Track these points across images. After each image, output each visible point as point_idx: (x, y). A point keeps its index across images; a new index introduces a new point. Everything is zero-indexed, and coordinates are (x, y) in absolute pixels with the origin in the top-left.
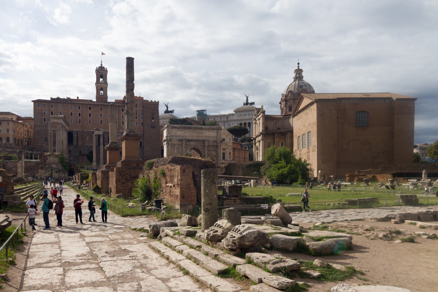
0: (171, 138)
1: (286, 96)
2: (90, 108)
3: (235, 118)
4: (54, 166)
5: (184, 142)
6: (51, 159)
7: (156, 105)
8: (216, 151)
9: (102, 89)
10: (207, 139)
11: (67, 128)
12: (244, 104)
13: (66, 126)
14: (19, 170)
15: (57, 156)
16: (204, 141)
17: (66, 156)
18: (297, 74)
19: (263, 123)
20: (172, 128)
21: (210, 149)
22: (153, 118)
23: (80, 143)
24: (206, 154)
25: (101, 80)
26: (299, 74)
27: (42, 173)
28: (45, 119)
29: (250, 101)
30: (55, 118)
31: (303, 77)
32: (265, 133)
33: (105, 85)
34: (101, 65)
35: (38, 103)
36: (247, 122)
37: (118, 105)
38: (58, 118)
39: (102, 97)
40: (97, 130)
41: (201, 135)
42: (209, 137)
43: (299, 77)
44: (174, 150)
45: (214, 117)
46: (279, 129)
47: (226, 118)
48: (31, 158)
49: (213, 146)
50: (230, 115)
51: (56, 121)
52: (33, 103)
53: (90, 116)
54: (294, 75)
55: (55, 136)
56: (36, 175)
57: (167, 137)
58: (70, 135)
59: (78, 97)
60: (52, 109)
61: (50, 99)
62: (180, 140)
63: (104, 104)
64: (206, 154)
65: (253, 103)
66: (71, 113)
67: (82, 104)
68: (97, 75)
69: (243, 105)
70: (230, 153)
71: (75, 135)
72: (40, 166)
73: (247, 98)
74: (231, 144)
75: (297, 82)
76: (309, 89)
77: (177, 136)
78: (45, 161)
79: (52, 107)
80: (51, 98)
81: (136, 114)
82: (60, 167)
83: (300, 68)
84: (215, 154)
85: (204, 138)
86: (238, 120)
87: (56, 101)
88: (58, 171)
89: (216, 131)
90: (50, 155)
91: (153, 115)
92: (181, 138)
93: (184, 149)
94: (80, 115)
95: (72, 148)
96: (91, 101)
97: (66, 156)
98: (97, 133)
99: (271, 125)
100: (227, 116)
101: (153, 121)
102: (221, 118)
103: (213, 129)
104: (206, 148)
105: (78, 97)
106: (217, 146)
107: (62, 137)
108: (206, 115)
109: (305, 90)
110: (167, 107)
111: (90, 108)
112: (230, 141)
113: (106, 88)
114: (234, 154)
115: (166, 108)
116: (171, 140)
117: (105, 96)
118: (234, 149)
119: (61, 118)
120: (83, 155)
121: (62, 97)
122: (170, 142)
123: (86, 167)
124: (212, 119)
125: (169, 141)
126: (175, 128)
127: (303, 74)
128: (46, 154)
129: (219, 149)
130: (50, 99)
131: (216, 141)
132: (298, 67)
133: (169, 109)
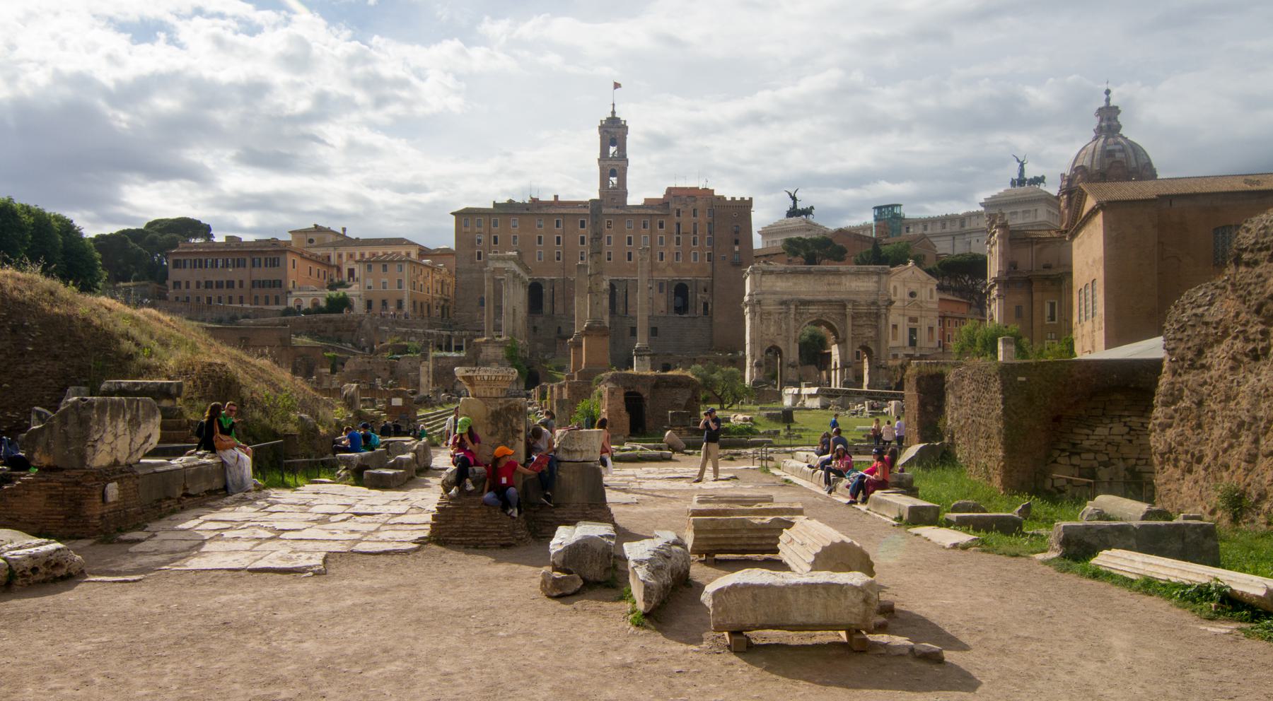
0: (760, 297)
1: (1070, 180)
5: (793, 307)
7: (744, 207)
8: (876, 327)
9: (613, 173)
10: (853, 297)
11: (527, 278)
12: (1013, 183)
13: (523, 274)
14: (423, 380)
15: (501, 345)
16: (842, 304)
17: (521, 342)
18: (1102, 120)
19: (1002, 254)
20: (764, 273)
21: (861, 323)
22: (737, 242)
23: (559, 308)
24: (850, 335)
25: (612, 149)
26: (1109, 119)
28: (479, 254)
29: (1029, 174)
30: (498, 259)
31: (1120, 127)
32: (1006, 278)
34: (613, 112)
35: (465, 217)
37: (650, 212)
38: (504, 259)
39: (613, 192)
41: (834, 288)
42: (858, 293)
43: (1109, 126)
44: (768, 327)
45: (925, 222)
46: (1048, 267)
47: (958, 224)
48: (448, 349)
49: (868, 315)
50: (969, 216)
51: (499, 265)
54: (1095, 122)
55: (498, 293)
57: (750, 295)
58: (535, 292)
59: (556, 197)
60: (496, 231)
62: (783, 303)
64: (850, 335)
65: (1040, 180)
66: (540, 238)
68: (602, 138)
69: (1009, 187)
70: (931, 329)
71: (546, 291)
73: (1022, 165)
74: (936, 306)
75: (1102, 140)
76: (1133, 159)
77: (775, 293)
79: (495, 225)
80: (495, 204)
81: (695, 232)
83: (1112, 103)
84: (872, 334)
85: (843, 297)
87: (507, 210)
89: (875, 278)
90: (487, 342)
91: (737, 232)
92: (785, 297)
93: (792, 323)
94: (558, 242)
95: (539, 320)
97: (521, 342)
99: (1025, 258)
100: (962, 219)
101: (737, 248)
102: (944, 226)
103: (868, 273)
104: (849, 321)
105: (556, 197)
106: (878, 316)
107: (516, 299)
108: (898, 218)
109: (1120, 162)
110: (794, 199)
112: (931, 297)
113: (625, 169)
115: (791, 202)
116: (759, 302)
117: (621, 191)
118: (943, 318)
119: (511, 258)
121: (518, 200)
122: (758, 309)
124: (915, 231)
125: (756, 304)
126: (771, 272)
127: (1120, 118)
128: (477, 340)
129: (883, 321)
131: (874, 303)
132: (1108, 100)
133: (800, 206)
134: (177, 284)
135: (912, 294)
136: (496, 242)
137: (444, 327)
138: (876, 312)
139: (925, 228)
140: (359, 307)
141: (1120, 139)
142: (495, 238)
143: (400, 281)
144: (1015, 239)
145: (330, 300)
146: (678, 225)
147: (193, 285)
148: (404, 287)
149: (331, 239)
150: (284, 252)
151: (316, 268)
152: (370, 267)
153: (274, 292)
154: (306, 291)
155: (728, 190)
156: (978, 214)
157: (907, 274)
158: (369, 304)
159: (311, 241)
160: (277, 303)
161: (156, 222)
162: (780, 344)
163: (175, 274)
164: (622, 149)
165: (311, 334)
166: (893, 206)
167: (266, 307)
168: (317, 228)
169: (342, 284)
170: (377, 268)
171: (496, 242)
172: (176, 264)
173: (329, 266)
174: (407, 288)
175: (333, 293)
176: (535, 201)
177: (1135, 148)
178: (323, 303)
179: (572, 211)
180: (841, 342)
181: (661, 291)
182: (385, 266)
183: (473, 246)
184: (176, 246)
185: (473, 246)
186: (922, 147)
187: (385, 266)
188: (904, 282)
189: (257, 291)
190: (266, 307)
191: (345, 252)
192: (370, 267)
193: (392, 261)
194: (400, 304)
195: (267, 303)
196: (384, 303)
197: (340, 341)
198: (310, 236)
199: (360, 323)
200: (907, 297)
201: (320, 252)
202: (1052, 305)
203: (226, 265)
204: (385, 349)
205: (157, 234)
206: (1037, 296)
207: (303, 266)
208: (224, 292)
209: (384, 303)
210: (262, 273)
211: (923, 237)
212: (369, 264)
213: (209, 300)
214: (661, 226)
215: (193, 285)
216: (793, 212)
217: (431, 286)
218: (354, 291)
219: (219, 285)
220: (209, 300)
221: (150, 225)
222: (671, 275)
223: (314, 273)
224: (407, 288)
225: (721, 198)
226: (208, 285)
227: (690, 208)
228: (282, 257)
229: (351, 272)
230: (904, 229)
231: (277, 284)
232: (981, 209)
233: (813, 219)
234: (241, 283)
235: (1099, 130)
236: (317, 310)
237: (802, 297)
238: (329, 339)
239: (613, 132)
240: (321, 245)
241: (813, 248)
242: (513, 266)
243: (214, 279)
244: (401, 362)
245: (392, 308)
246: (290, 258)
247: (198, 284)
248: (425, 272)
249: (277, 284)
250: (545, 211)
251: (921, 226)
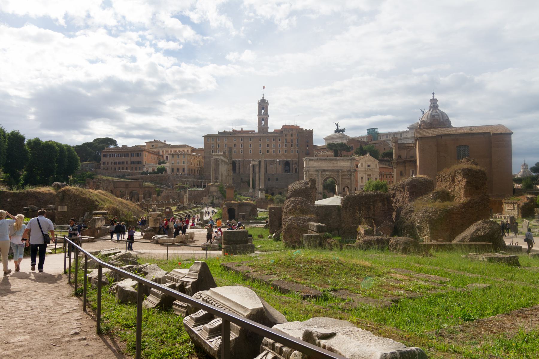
2: (251, 140)
4: (215, 194)
5: (320, 172)
6: (213, 189)
7: (310, 133)
8: (351, 179)
9: (263, 120)
10: (341, 168)
14: (185, 200)
15: (217, 186)
16: (338, 171)
20: (310, 160)
22: (307, 146)
24: (340, 182)
27: (206, 200)
30: (216, 155)
33: (266, 116)
34: (263, 98)
35: (208, 138)
37: (275, 135)
38: (218, 155)
40: (253, 160)
41: (334, 165)
43: (434, 106)
48: (201, 187)
50: (404, 132)
51: (216, 157)
53: (250, 146)
56: (202, 201)
59: (242, 129)
60: (219, 142)
61: (217, 133)
62: (317, 171)
63: (265, 135)
64: (340, 182)
72: (205, 194)
76: (441, 118)
77: (314, 167)
78: (208, 190)
80: (219, 133)
82: (220, 195)
83: (435, 97)
85: (338, 168)
87: (224, 135)
88: (218, 198)
89: (350, 162)
90: (212, 185)
91: (307, 142)
92: (317, 169)
93: (320, 178)
96: (253, 132)
98: (253, 163)
101: (307, 148)
103: (347, 160)
105: (242, 129)
106: (351, 175)
107: (224, 169)
108: (377, 133)
110: (337, 126)
111: (251, 140)
113: (268, 119)
115: (336, 127)
116: (308, 170)
117: (266, 127)
118: (381, 175)
119: (221, 155)
120: (244, 182)
121: (227, 131)
122: (307, 173)
123: (244, 193)
124: (383, 138)
126: (312, 160)
127: (438, 103)
130: (217, 133)
131: (349, 171)
132: (433, 96)
133: (340, 128)
134: (104, 163)
135: (369, 166)
137: (200, 178)
138: (352, 173)
139: (387, 137)
140: (169, 171)
141: (437, 111)
143: (184, 161)
144: (401, 147)
145: (158, 169)
146: (286, 140)
147: (110, 163)
148: (184, 163)
149: (160, 145)
150: (143, 151)
151: (154, 156)
152: (173, 156)
153: (138, 166)
154: (150, 165)
155: (305, 126)
156: (407, 132)
157: (367, 158)
158: (173, 170)
159: (153, 146)
160: (140, 170)
161: (97, 139)
163: (103, 160)
164: (266, 111)
165: (151, 182)
166: (374, 129)
167: (136, 171)
168: (155, 141)
169: (164, 163)
170: (176, 157)
172: (104, 156)
173: (159, 155)
174: (186, 164)
175: (160, 166)
177: (443, 114)
178: (156, 170)
179: (247, 135)
180: (338, 185)
181: (279, 164)
182: (178, 156)
184: (104, 149)
186: (397, 101)
187: (178, 156)
188: (365, 161)
189: (133, 165)
190: (136, 171)
191: (165, 150)
192: (173, 156)
193: (181, 154)
194: (184, 170)
195: (136, 170)
196: (178, 169)
197: (161, 184)
198: (152, 144)
199: (169, 177)
200: (367, 167)
201: (156, 150)
202: (413, 171)
203: (122, 156)
204: (176, 188)
205: (97, 144)
206: (407, 168)
207: (149, 156)
208: (121, 166)
209: (178, 169)
210: (135, 159)
211: (384, 141)
212: (173, 155)
213: (115, 169)
214: (279, 140)
215: (110, 163)
216: (337, 131)
217: (195, 163)
218: (167, 165)
219: (119, 163)
220: (115, 169)
221: (95, 140)
222: (283, 158)
223: (153, 158)
224: (186, 164)
225: (302, 129)
226: (115, 163)
227: (290, 133)
228: (142, 153)
229: (167, 157)
230: (379, 138)
231: (140, 163)
232: (408, 130)
233: (346, 133)
234: (127, 162)
235: (431, 107)
236: (154, 172)
237: (324, 168)
238: (158, 183)
239: (263, 105)
240: (156, 148)
241: (340, 147)
242: (222, 158)
243: (117, 161)
245: (181, 171)
246: (145, 153)
247: (112, 163)
248: (193, 158)
249: (140, 163)
250: (237, 135)
251: (385, 136)
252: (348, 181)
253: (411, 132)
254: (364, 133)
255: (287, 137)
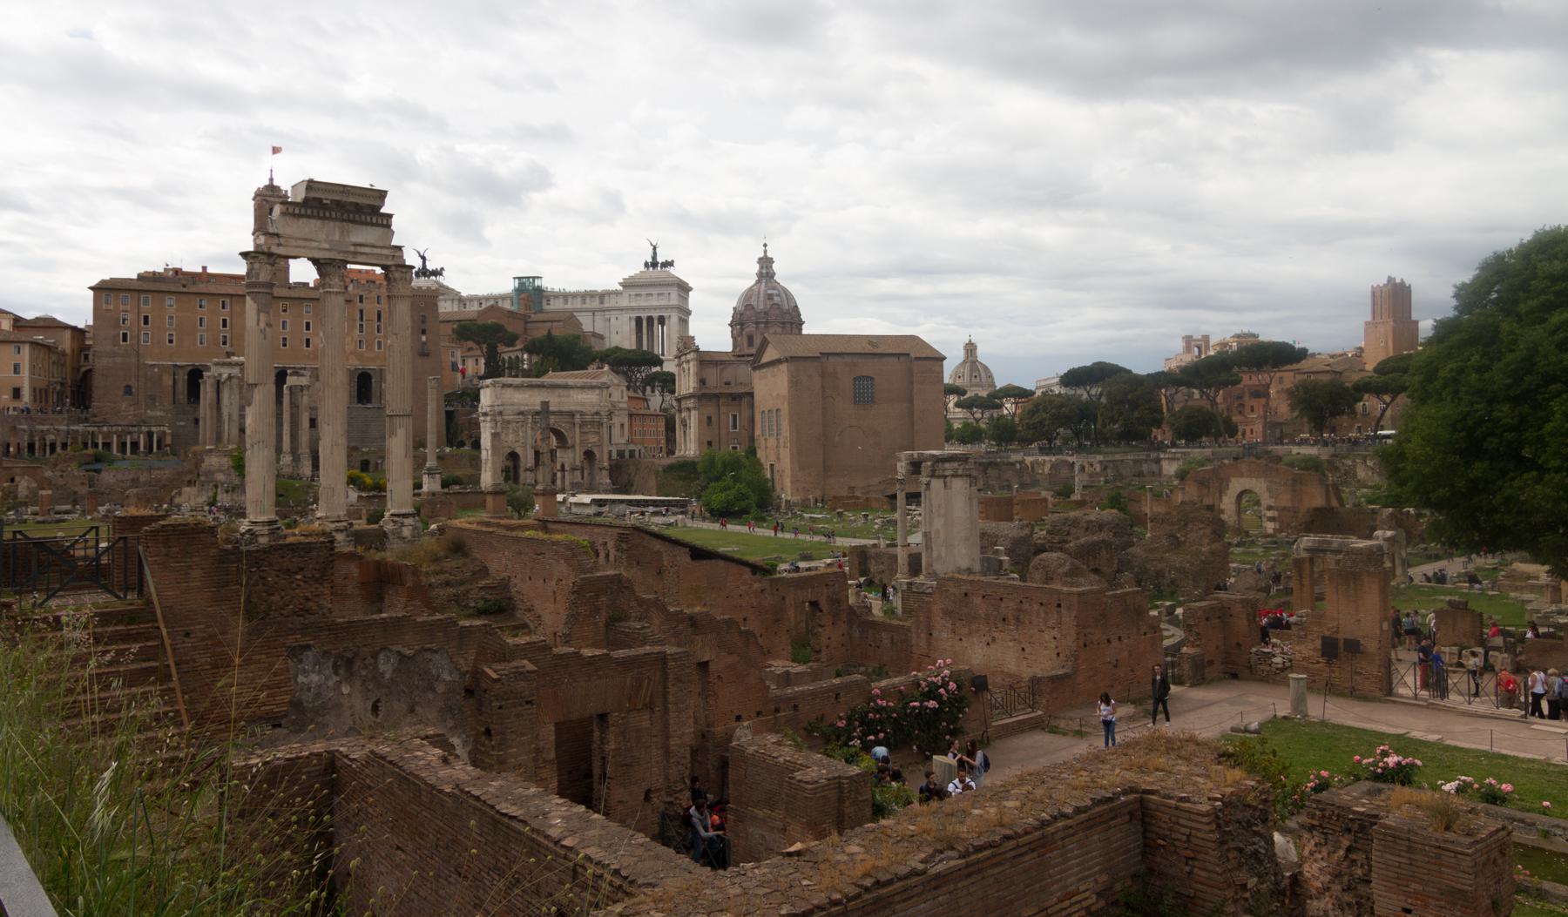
3: (624, 302)
10: (579, 408)
12: (646, 265)
16: (572, 414)
20: (504, 386)
22: (424, 332)
28: (125, 335)
35: (103, 290)
36: (655, 315)
42: (583, 404)
47: (597, 300)
52: (91, 293)
59: (204, 268)
60: (146, 309)
62: (521, 413)
65: (669, 264)
67: (232, 295)
69: (642, 268)
72: (188, 478)
78: (197, 466)
79: (146, 303)
85: (573, 408)
86: (632, 309)
94: (225, 325)
101: (424, 338)
105: (204, 268)
108: (539, 290)
110: (424, 258)
114: (631, 425)
116: (501, 413)
118: (631, 415)
124: (556, 305)
126: (510, 386)
131: (597, 413)
133: (430, 266)
136: (146, 322)
142: (146, 318)
156: (616, 293)
162: (519, 451)
171: (146, 322)
176: (177, 271)
183: (117, 326)
185: (117, 326)
222: (355, 363)
227: (374, 294)
244: (103, 474)
252: (593, 439)
253: (626, 295)
254: (507, 286)
255: (366, 306)
